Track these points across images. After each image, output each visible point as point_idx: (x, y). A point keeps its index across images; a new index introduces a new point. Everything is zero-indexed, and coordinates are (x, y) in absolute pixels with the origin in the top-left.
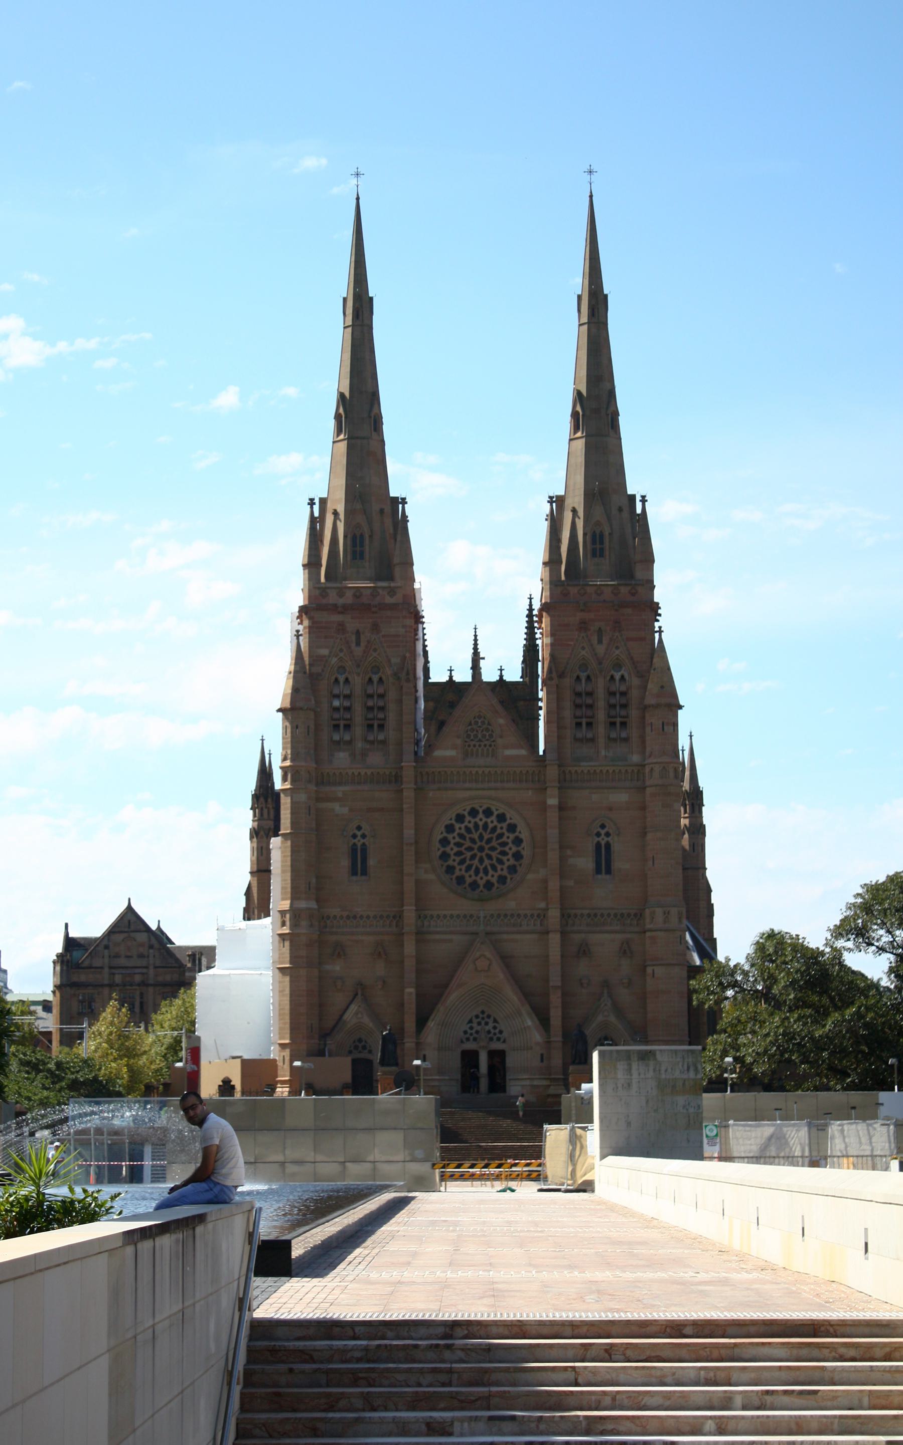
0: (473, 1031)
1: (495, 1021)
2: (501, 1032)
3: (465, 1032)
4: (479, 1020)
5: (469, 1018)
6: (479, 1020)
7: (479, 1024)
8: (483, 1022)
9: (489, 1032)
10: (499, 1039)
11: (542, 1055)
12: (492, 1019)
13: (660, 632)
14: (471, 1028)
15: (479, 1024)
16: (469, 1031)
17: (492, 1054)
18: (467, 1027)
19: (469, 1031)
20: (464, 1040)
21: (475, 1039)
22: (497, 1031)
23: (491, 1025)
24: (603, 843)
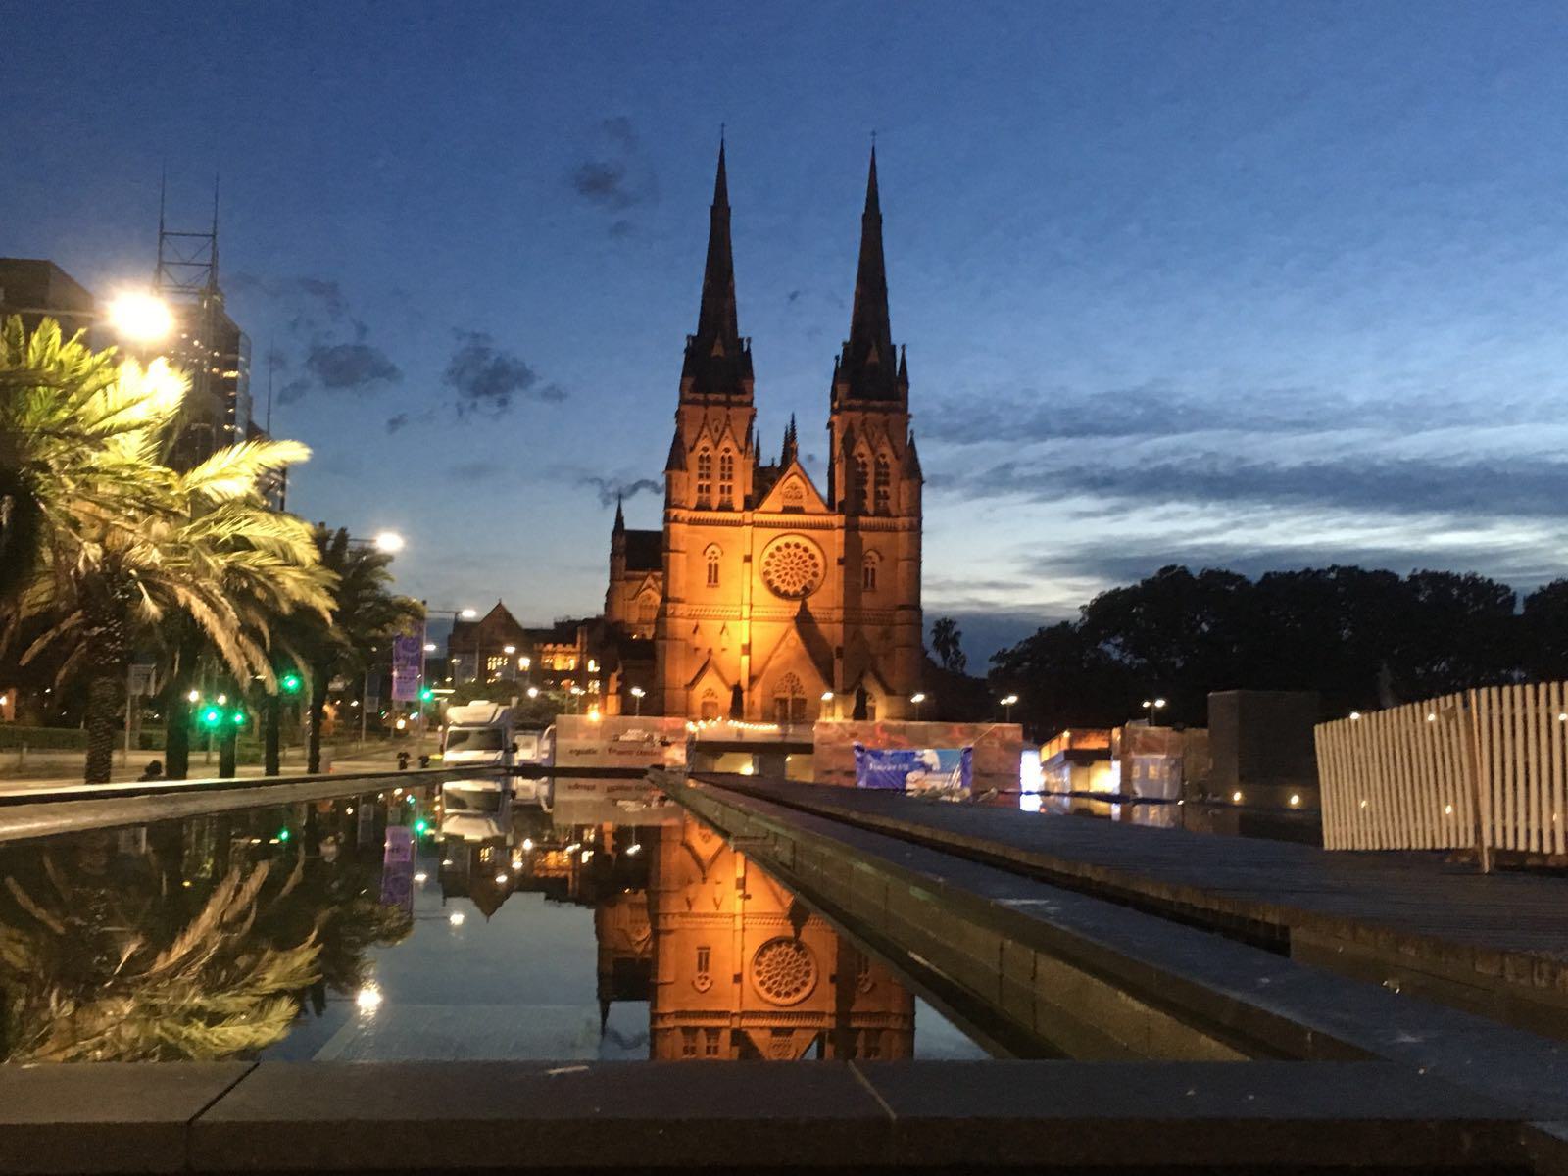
13: (912, 432)
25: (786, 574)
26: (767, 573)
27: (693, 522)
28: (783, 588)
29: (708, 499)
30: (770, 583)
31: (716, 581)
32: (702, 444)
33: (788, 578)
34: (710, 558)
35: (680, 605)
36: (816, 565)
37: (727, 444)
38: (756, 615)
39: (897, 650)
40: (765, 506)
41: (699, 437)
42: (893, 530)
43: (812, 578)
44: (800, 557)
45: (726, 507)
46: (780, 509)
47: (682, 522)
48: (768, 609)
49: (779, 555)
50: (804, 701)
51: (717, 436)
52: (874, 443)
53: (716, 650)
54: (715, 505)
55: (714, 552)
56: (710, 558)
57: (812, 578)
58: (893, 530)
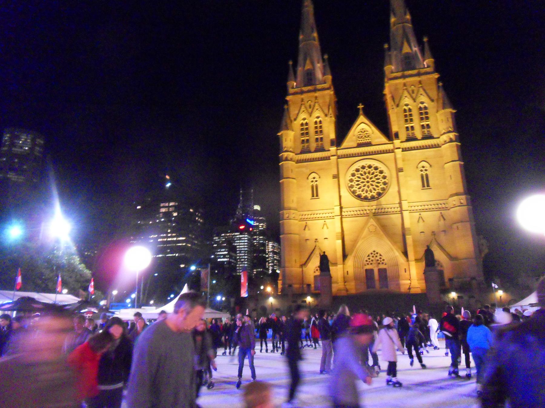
1: (380, 255)
7: (373, 257)
8: (375, 256)
9: (378, 260)
10: (383, 263)
11: (405, 269)
14: (369, 259)
15: (373, 257)
17: (380, 270)
18: (367, 258)
21: (371, 264)
25: (364, 186)
26: (352, 186)
27: (298, 162)
28: (364, 195)
29: (308, 146)
30: (354, 192)
31: (317, 196)
32: (302, 116)
33: (366, 188)
34: (312, 181)
35: (292, 211)
36: (384, 177)
37: (317, 113)
38: (346, 213)
39: (455, 226)
40: (345, 144)
41: (299, 112)
42: (437, 146)
43: (383, 186)
44: (373, 174)
45: (321, 149)
46: (356, 145)
47: (291, 160)
48: (354, 209)
49: (358, 174)
50: (385, 270)
51: (310, 110)
52: (414, 95)
53: (320, 239)
54: (313, 149)
55: (314, 178)
56: (312, 181)
57: (383, 186)
58: (437, 146)
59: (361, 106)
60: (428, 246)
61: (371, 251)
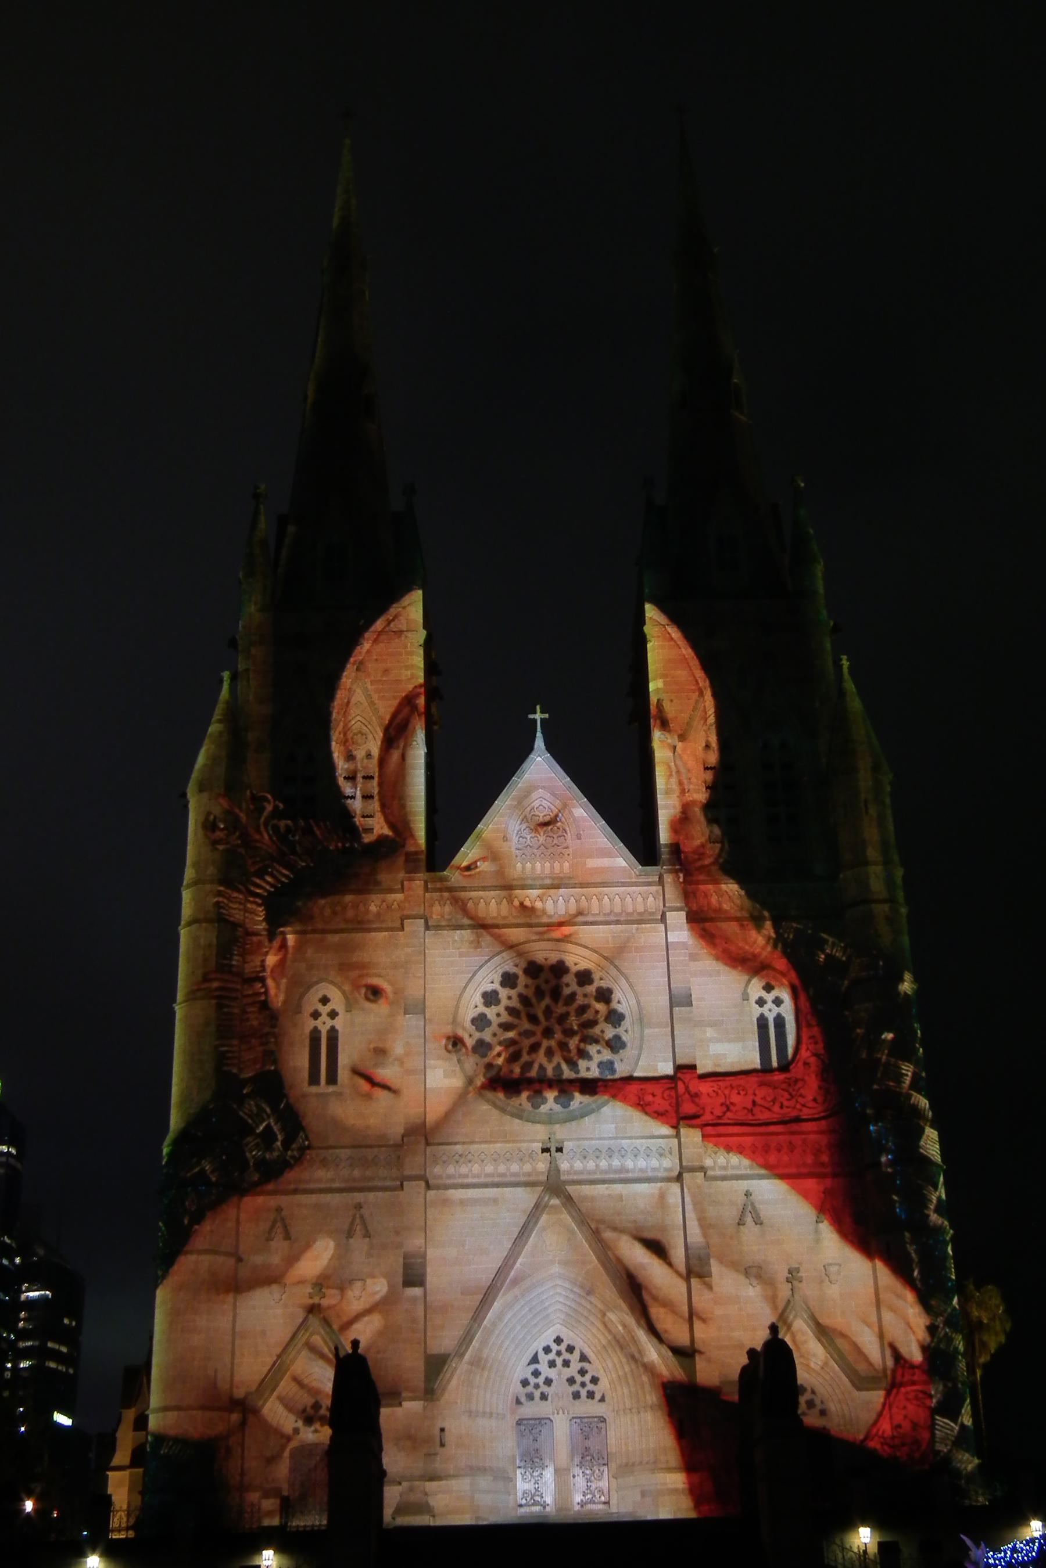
0: (541, 1380)
1: (583, 1358)
2: (595, 1380)
3: (525, 1383)
4: (552, 1356)
5: (529, 1355)
6: (552, 1356)
7: (552, 1364)
8: (559, 1361)
10: (591, 1395)
12: (576, 1354)
14: (536, 1374)
15: (552, 1364)
16: (532, 1380)
19: (532, 1380)
20: (523, 1399)
22: (587, 1378)
23: (575, 1366)
24: (771, 1017)
59: (538, 716)
60: (774, 1329)
61: (547, 1338)
